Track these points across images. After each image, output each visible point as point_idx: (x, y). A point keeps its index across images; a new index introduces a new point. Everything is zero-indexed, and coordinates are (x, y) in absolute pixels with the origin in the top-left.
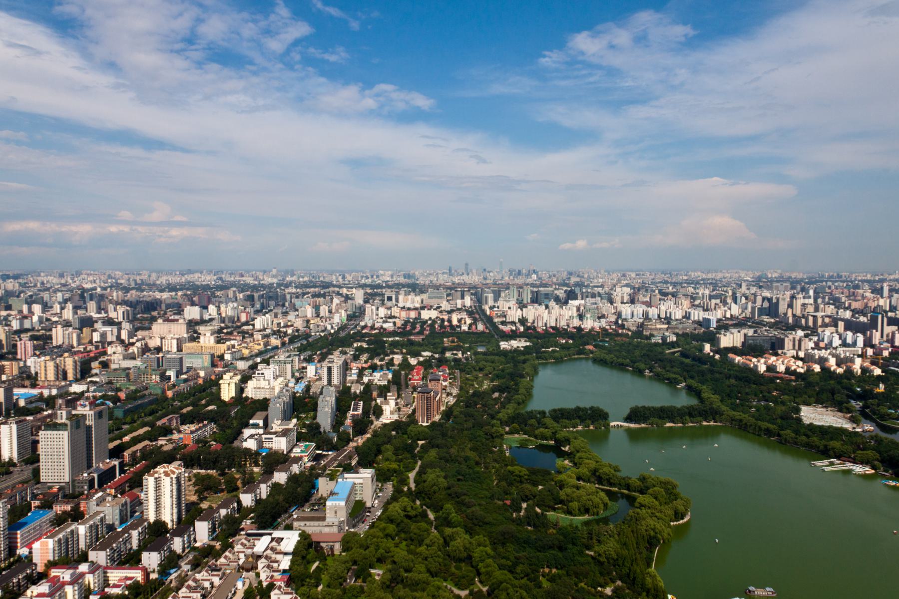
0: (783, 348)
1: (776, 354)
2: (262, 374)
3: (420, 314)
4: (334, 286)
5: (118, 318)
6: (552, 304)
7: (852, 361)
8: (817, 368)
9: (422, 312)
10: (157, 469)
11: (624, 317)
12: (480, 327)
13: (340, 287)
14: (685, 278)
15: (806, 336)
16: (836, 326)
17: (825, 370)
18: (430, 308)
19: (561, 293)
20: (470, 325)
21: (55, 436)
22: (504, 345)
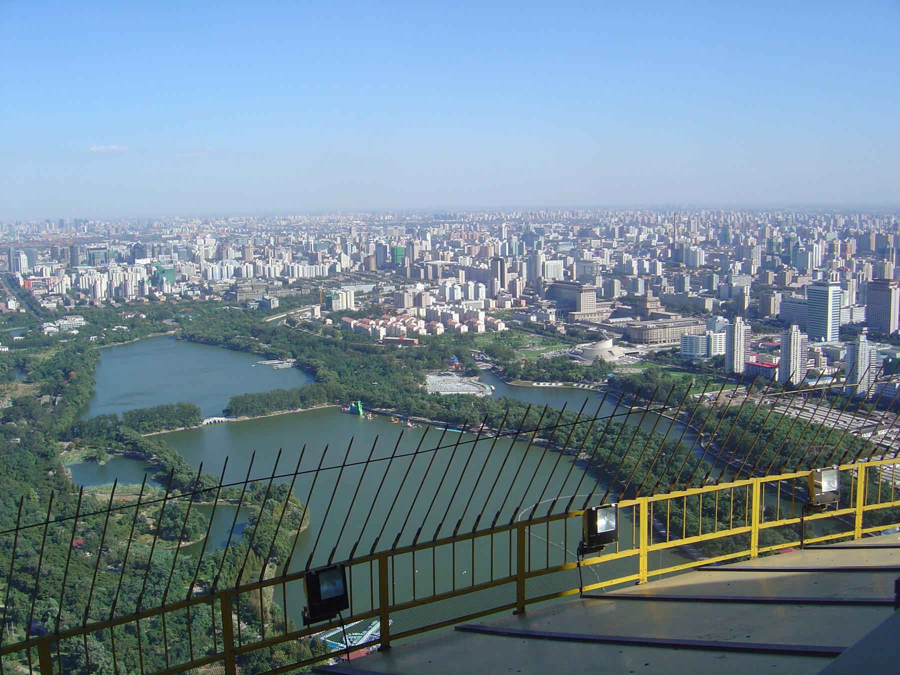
0: (403, 307)
1: (395, 314)
6: (113, 265)
7: (476, 315)
8: (440, 329)
11: (210, 278)
14: (284, 223)
15: (427, 290)
16: (457, 276)
17: (449, 328)
19: (124, 250)
22: (50, 328)
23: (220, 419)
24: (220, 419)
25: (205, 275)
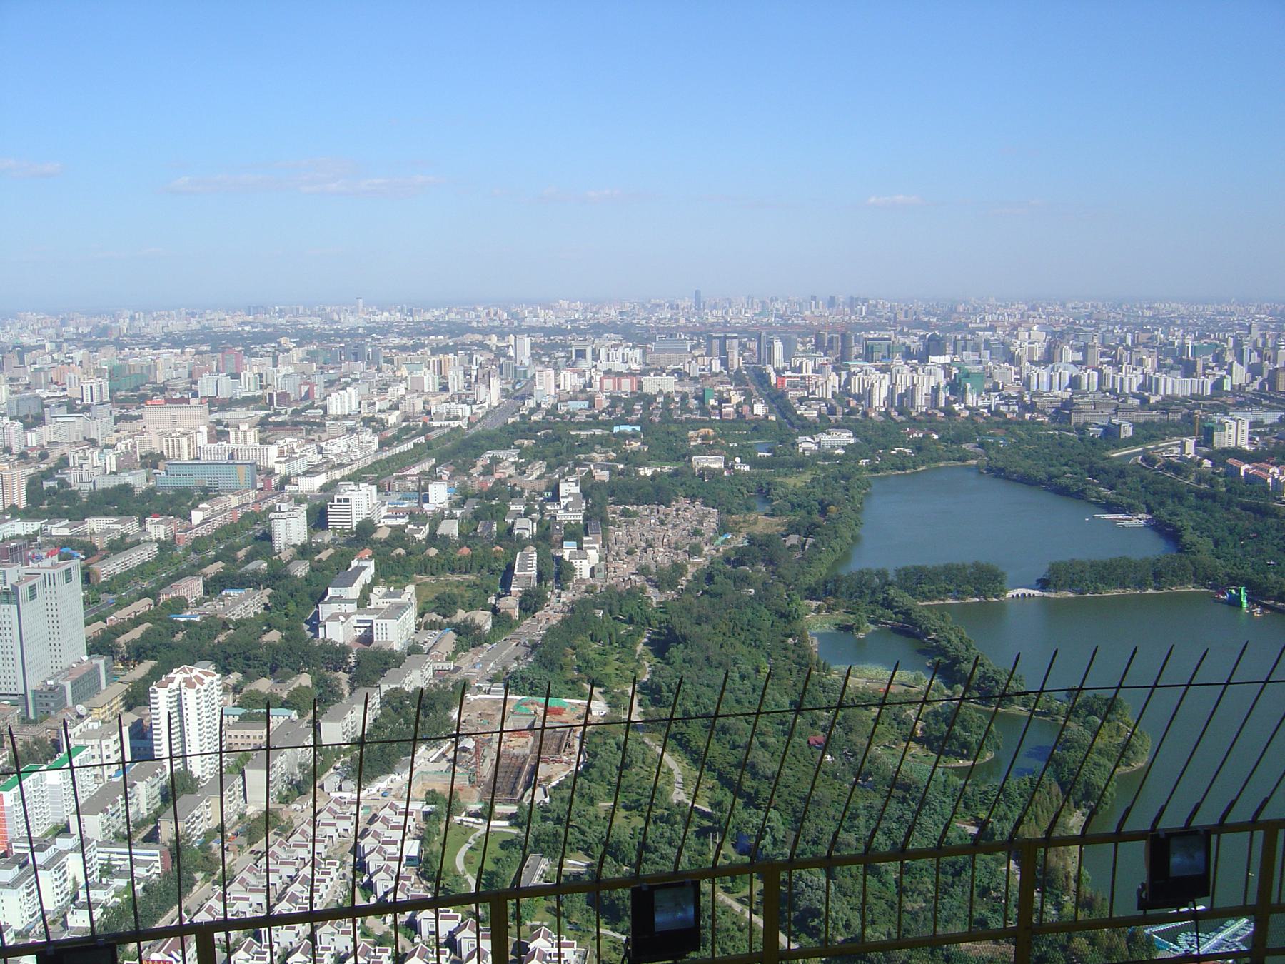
2: (346, 500)
3: (640, 383)
4: (474, 331)
5: (82, 400)
6: (898, 362)
9: (644, 379)
10: (171, 675)
11: (1034, 388)
12: (759, 409)
13: (486, 332)
14: (1148, 313)
18: (660, 371)
19: (914, 342)
20: (739, 405)
22: (806, 444)
23: (1032, 592)
24: (1032, 592)
25: (1027, 384)
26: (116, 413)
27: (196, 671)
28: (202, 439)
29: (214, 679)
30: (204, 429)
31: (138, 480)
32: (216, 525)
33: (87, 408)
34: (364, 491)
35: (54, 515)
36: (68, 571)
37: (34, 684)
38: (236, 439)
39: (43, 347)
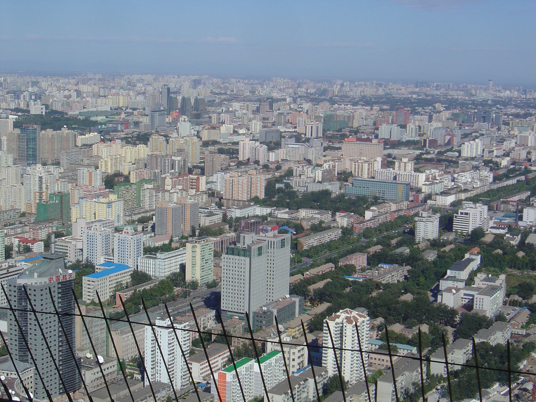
2: (466, 214)
5: (305, 135)
10: (338, 314)
21: (237, 261)
26: (325, 144)
27: (354, 313)
28: (378, 165)
29: (365, 319)
30: (379, 159)
31: (335, 188)
32: (380, 221)
33: (308, 140)
34: (479, 209)
35: (279, 205)
36: (283, 242)
37: (254, 308)
38: (399, 167)
39: (285, 100)
